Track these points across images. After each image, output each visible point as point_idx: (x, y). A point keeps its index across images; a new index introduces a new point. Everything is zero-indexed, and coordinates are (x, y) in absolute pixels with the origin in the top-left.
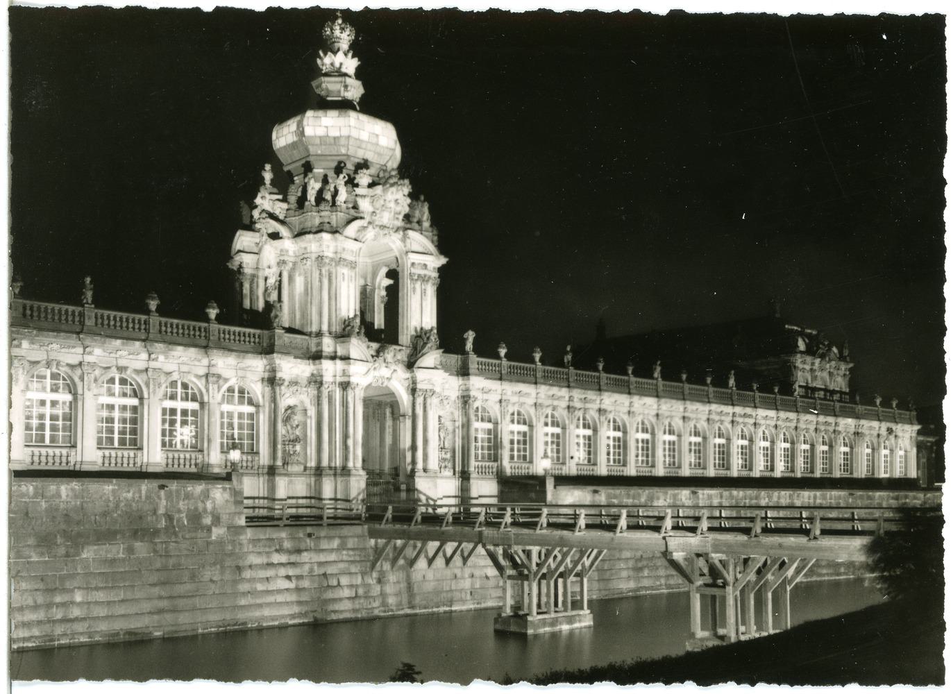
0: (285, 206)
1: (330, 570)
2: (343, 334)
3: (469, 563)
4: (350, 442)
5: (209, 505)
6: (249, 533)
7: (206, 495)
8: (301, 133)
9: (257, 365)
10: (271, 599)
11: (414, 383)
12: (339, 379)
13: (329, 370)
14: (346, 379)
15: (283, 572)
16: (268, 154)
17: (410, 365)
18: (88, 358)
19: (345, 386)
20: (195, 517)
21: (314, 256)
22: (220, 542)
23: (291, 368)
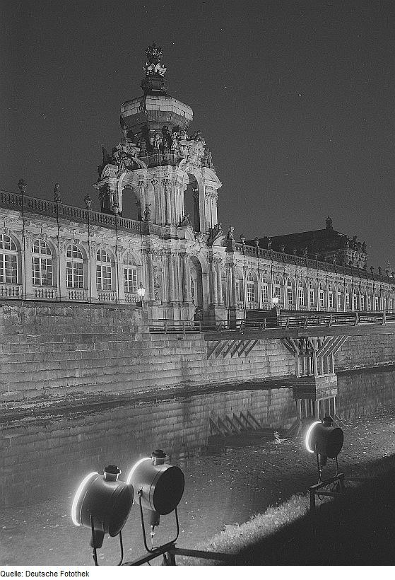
1: (191, 358)
2: (182, 225)
3: (249, 355)
4: (186, 287)
5: (133, 321)
6: (152, 337)
7: (130, 316)
8: (143, 106)
10: (165, 375)
11: (211, 254)
12: (179, 251)
15: (169, 360)
17: (210, 244)
18: (61, 234)
19: (183, 255)
20: (127, 328)
22: (139, 343)
23: (156, 243)
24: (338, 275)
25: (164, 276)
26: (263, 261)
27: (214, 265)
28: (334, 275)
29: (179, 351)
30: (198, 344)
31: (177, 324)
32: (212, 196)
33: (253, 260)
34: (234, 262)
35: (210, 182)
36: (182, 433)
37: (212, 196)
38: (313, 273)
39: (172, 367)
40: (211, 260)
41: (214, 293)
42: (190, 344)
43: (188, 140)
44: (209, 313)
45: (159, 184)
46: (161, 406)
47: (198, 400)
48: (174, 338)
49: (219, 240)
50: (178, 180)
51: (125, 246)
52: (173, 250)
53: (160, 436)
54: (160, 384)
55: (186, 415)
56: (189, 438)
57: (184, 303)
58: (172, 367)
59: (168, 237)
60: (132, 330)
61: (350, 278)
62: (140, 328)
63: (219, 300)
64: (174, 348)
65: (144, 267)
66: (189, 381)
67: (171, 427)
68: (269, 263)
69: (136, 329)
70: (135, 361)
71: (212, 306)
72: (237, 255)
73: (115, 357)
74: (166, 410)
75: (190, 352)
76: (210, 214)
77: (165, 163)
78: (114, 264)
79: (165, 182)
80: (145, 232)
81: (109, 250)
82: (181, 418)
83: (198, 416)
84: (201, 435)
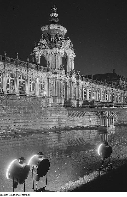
0: (47, 42)
1: (62, 117)
3: (83, 117)
6: (48, 109)
8: (49, 27)
9: (45, 75)
11: (71, 80)
12: (59, 78)
13: (57, 76)
14: (61, 78)
15: (54, 117)
16: (41, 32)
19: (61, 80)
21: (54, 53)
22: (44, 111)
23: (52, 75)
24: (117, 89)
25: (54, 87)
26: (90, 83)
27: (72, 84)
28: (115, 89)
29: (58, 115)
30: (65, 112)
31: (58, 104)
32: (72, 59)
33: (86, 83)
34: (79, 83)
35: (72, 55)
36: (57, 145)
37: (72, 59)
38: (108, 88)
39: (55, 120)
40: (71, 82)
41: (71, 94)
42: (62, 112)
43: (64, 40)
44: (69, 101)
45: (54, 55)
46: (50, 135)
47: (64, 133)
48: (56, 109)
49: (74, 75)
50: (60, 53)
51: (40, 76)
52: (57, 78)
53: (49, 146)
54: (50, 126)
55: (59, 138)
56: (60, 147)
57: (60, 97)
58: (55, 120)
59: (56, 73)
60: (41, 106)
61: (121, 91)
62: (44, 106)
63: (73, 97)
64: (56, 113)
65: (47, 84)
66: (61, 126)
67: (53, 143)
68: (92, 84)
69: (43, 106)
70: (41, 117)
71: (70, 99)
72: (80, 81)
73: (34, 116)
74: (52, 136)
75: (62, 115)
76: (71, 65)
77: (56, 47)
78: (36, 82)
79: (56, 54)
80: (48, 71)
81: (34, 77)
82: (57, 139)
83: (64, 139)
84: (64, 146)
